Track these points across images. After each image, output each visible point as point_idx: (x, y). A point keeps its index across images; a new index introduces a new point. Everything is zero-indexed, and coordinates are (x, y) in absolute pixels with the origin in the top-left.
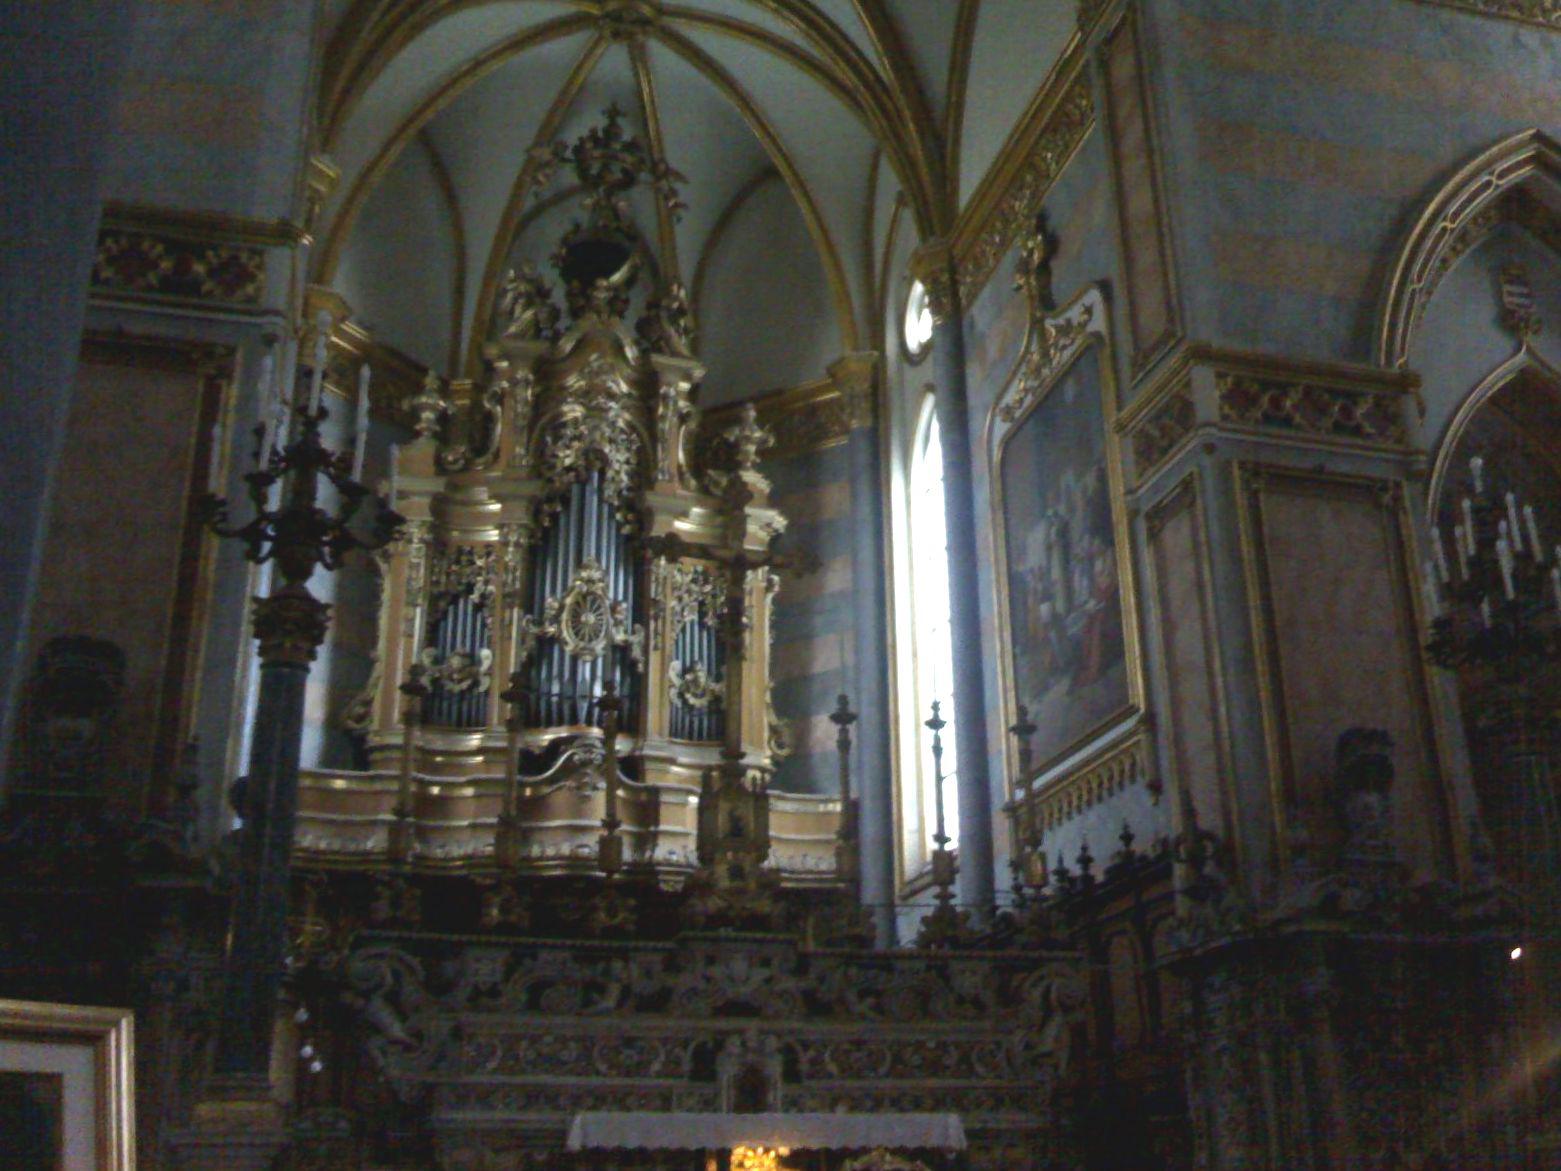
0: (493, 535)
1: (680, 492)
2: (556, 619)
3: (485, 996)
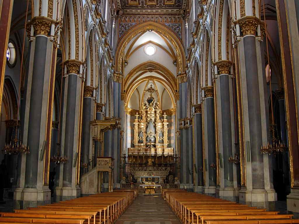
1: (159, 121)
2: (148, 134)
3: (137, 170)
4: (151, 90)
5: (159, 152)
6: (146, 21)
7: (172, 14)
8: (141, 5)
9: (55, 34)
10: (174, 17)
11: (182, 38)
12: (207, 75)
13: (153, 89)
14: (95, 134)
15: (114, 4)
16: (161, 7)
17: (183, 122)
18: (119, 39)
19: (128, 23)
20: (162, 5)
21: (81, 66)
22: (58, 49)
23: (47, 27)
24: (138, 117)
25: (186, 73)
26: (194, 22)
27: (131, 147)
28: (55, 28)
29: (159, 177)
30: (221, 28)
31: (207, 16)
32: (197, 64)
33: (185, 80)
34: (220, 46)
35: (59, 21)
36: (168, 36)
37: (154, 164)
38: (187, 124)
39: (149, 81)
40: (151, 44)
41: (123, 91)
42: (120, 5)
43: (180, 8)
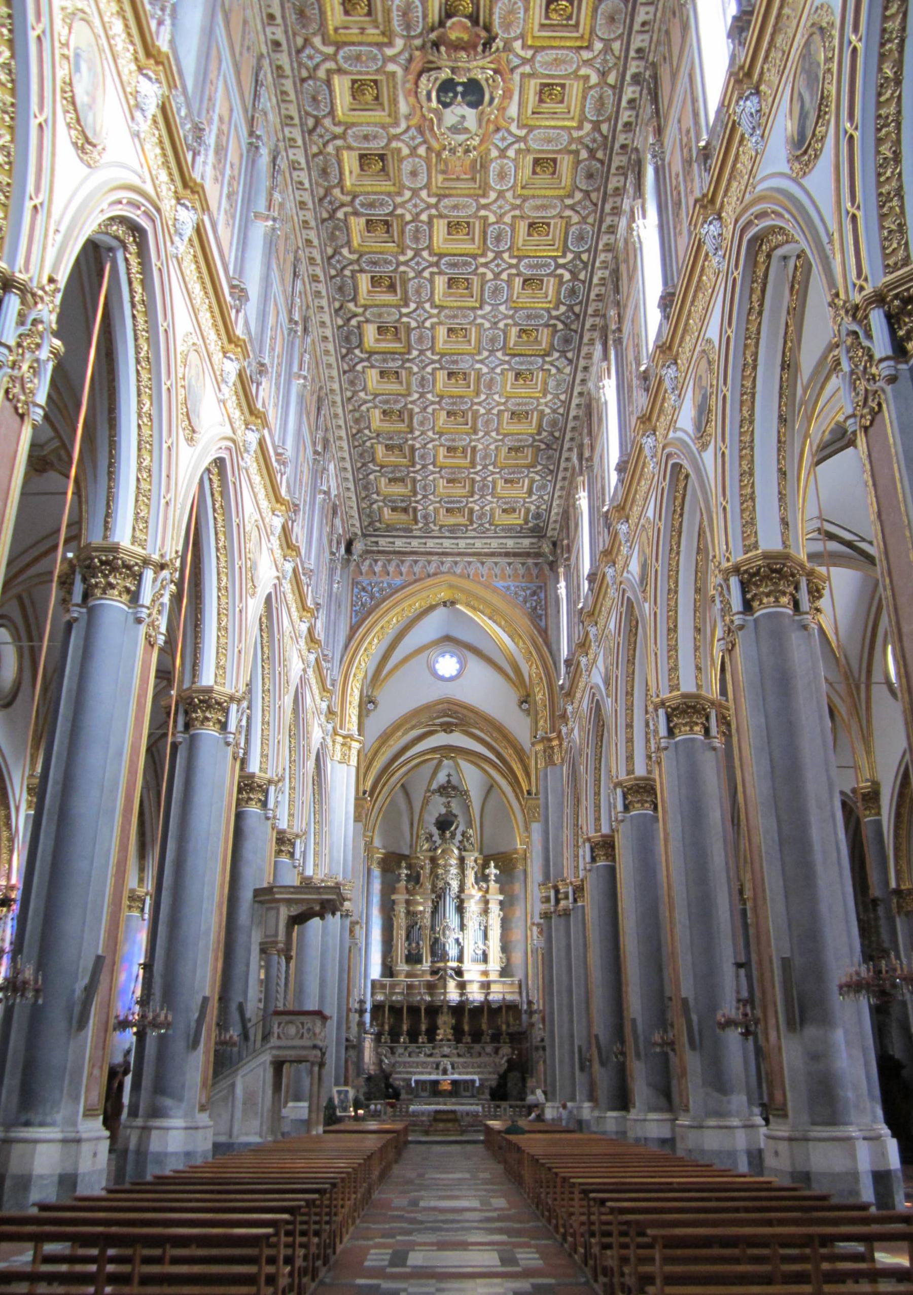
0: (421, 908)
3: (400, 1055)
4: (447, 789)
5: (475, 994)
6: (435, 574)
7: (516, 555)
8: (421, 525)
9: (153, 601)
10: (523, 564)
11: (546, 625)
12: (630, 740)
13: (454, 788)
14: (268, 933)
15: (338, 522)
16: (482, 534)
17: (552, 894)
18: (351, 628)
19: (380, 580)
20: (487, 526)
21: (234, 707)
22: (161, 650)
23: (128, 576)
24: (407, 875)
25: (559, 737)
26: (589, 576)
27: (383, 975)
28: (155, 580)
29: (476, 1077)
30: (676, 592)
31: (628, 558)
32: (597, 709)
33: (557, 759)
34: (673, 649)
35: (168, 558)
36: (503, 623)
37: (458, 1032)
38: (567, 898)
39: (441, 762)
40: (450, 647)
41: (361, 794)
42: (358, 525)
43: (543, 537)
